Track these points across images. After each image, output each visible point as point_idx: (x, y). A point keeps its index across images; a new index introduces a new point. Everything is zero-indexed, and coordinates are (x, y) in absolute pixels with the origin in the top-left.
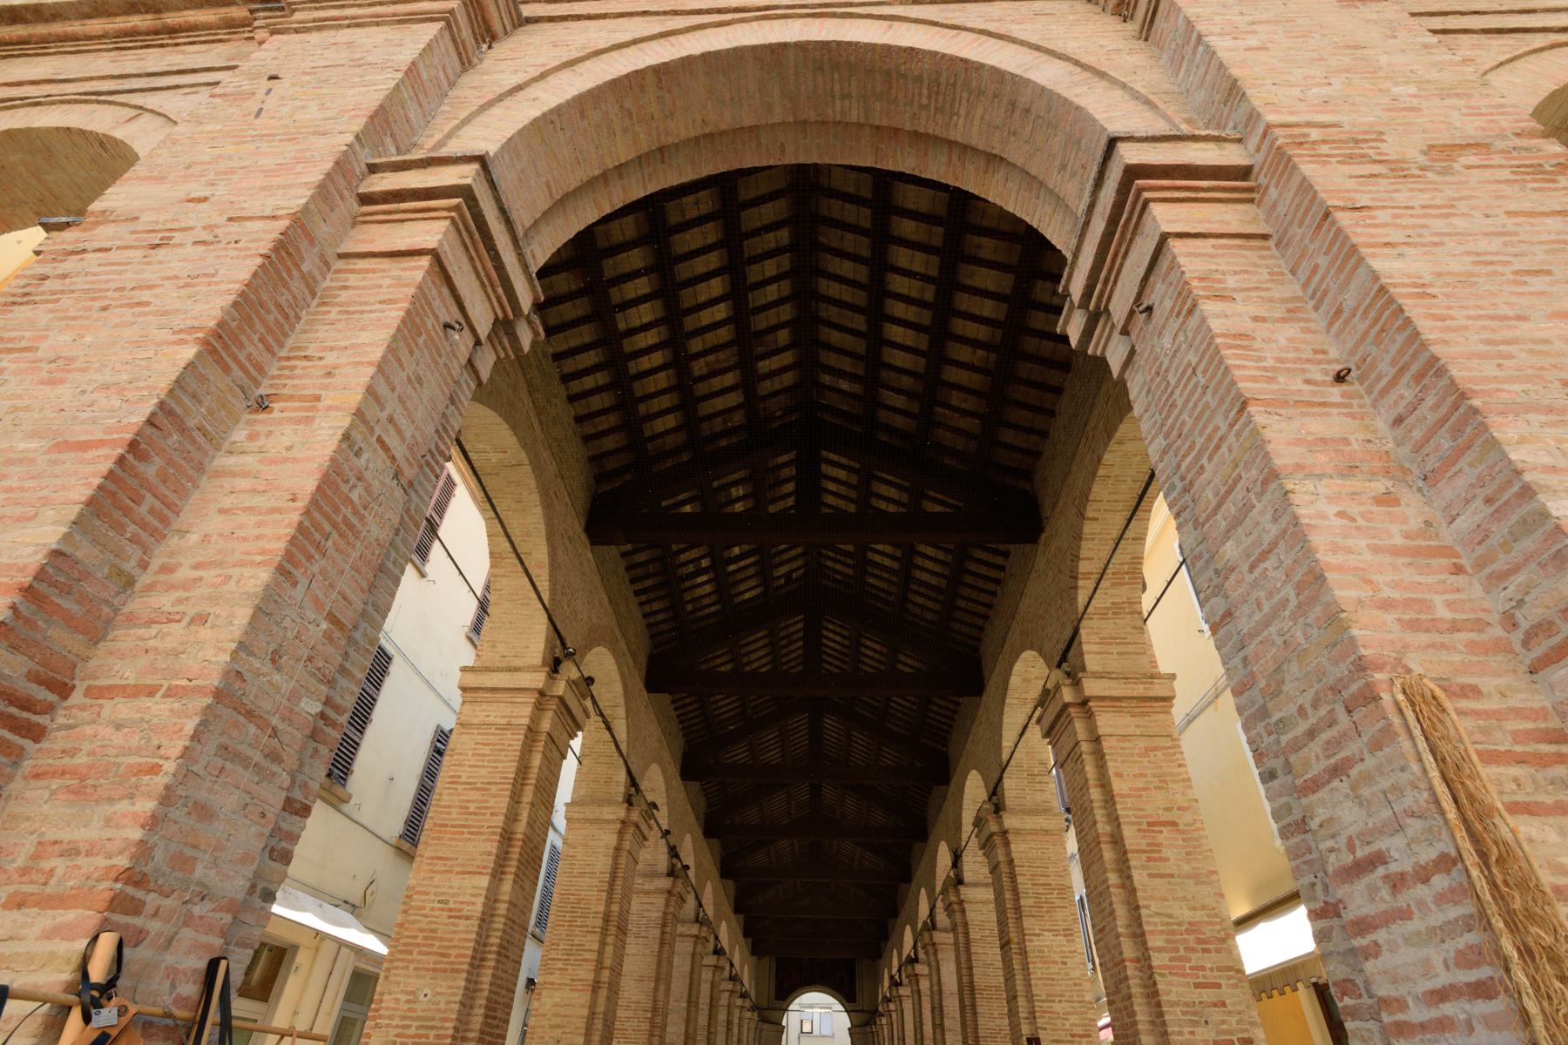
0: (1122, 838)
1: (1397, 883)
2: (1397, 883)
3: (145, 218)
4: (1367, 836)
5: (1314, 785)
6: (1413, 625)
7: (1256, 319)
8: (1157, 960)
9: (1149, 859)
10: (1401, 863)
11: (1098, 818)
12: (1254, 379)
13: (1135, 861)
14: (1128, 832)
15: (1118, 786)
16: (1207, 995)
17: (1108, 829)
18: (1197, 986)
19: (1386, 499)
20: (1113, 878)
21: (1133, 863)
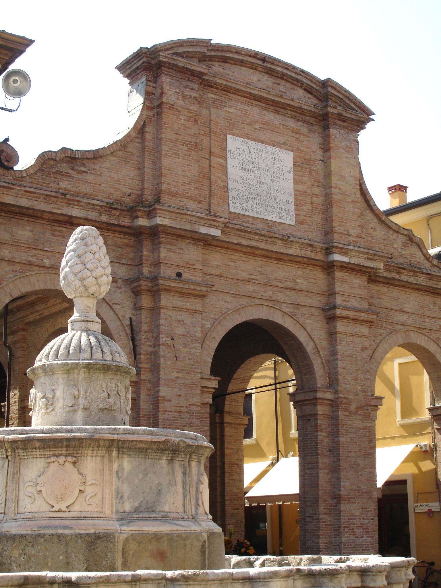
0: (224, 468)
1: (313, 519)
2: (313, 519)
3: (173, 401)
4: (312, 514)
5: (308, 506)
6: (324, 493)
7: (324, 437)
8: (227, 502)
9: (230, 475)
10: (314, 518)
11: (218, 461)
12: (320, 450)
13: (227, 475)
14: (226, 466)
15: (227, 452)
16: (236, 511)
17: (220, 464)
18: (235, 509)
19: (328, 474)
20: (218, 479)
21: (226, 476)
